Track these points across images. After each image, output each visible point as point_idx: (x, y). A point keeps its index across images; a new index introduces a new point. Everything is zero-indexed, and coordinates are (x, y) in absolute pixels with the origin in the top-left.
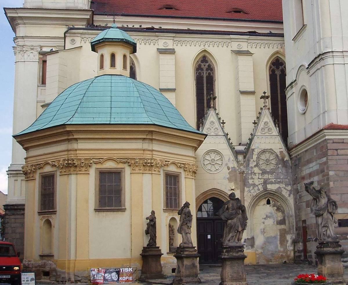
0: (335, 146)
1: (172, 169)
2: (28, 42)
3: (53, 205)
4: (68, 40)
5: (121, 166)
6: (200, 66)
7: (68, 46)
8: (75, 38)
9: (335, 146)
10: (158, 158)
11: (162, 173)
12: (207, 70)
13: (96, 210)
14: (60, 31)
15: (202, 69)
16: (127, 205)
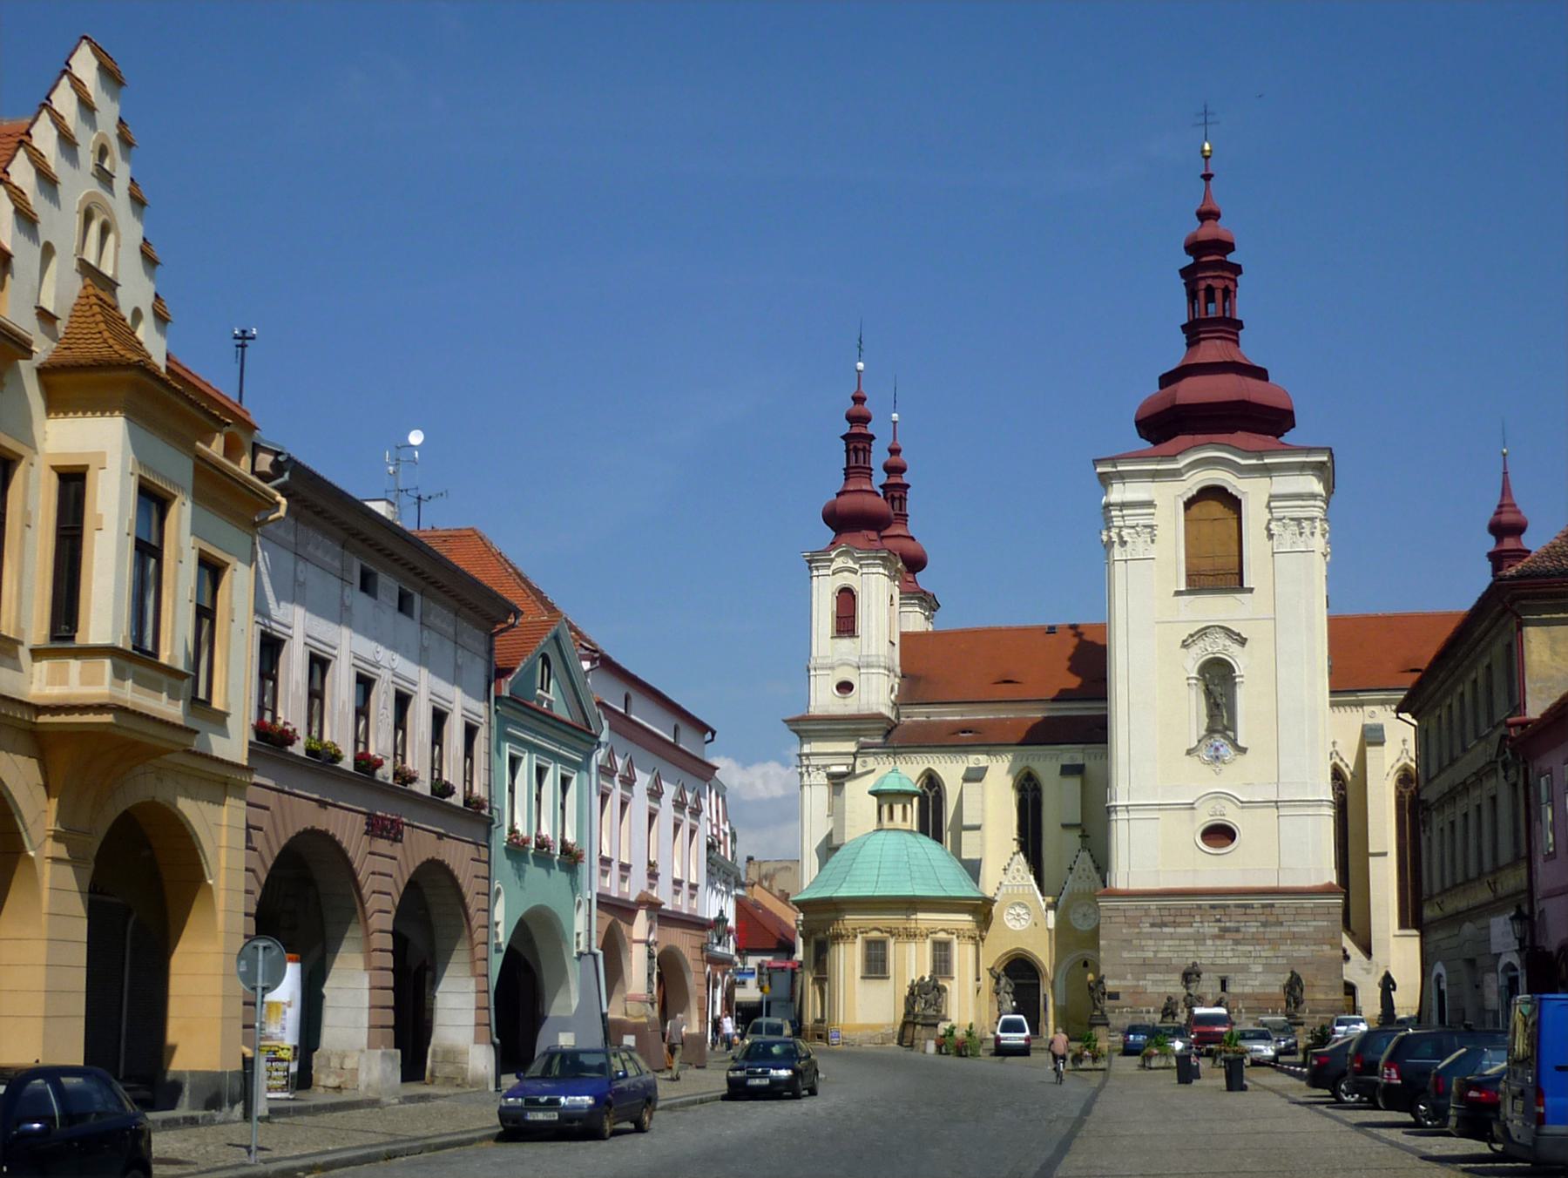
0: (1110, 913)
1: (942, 936)
2: (814, 761)
3: (825, 969)
4: (859, 761)
5: (885, 935)
6: (1023, 785)
7: (859, 770)
8: (867, 759)
9: (1110, 913)
10: (923, 926)
11: (928, 942)
12: (1032, 791)
13: (863, 978)
14: (851, 747)
15: (1026, 791)
16: (892, 972)
